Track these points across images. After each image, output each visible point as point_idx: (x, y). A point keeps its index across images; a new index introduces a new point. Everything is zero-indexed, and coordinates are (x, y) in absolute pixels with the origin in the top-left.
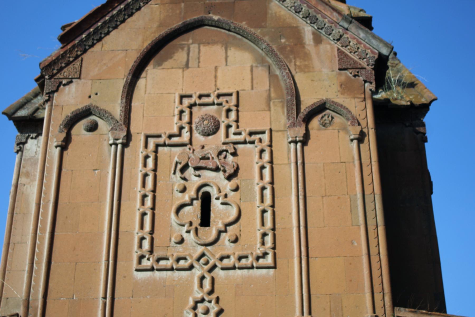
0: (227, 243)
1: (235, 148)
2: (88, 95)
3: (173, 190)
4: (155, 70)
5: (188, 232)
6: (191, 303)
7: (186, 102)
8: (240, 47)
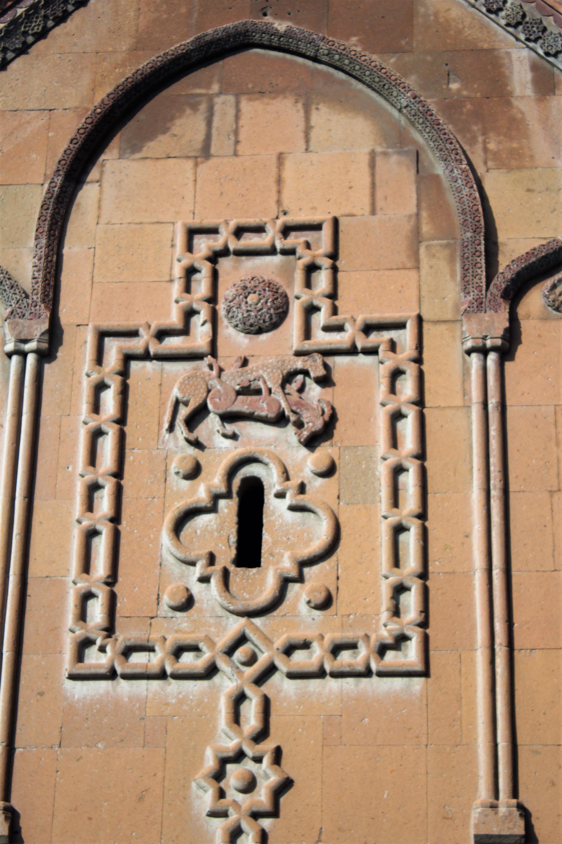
0: (303, 608)
1: (326, 366)
3: (166, 471)
4: (124, 163)
5: (204, 580)
6: (210, 763)
7: (203, 245)
8: (344, 102)
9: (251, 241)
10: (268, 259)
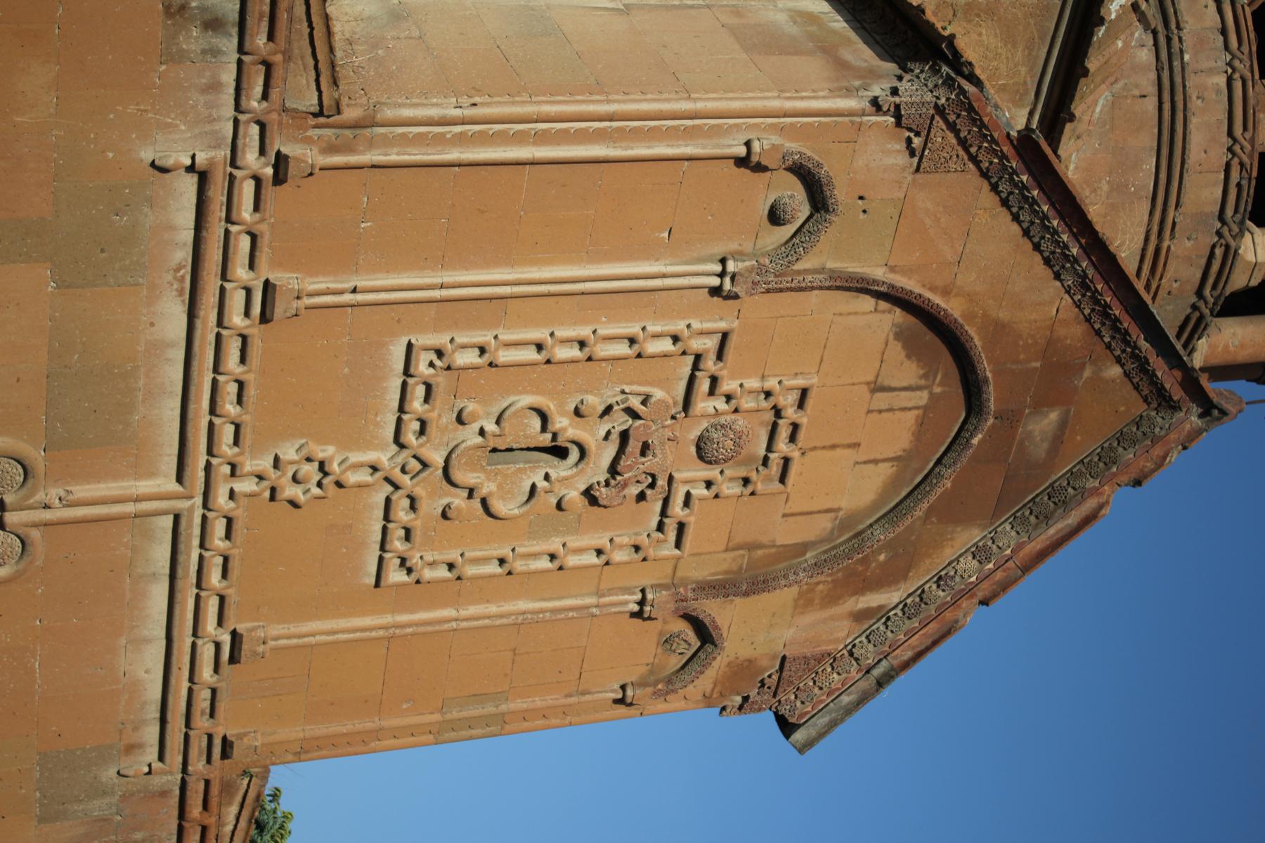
0: (445, 501)
2: (866, 195)
3: (587, 392)
6: (321, 456)
7: (788, 401)
8: (893, 484)
9: (784, 432)
10: (764, 446)
